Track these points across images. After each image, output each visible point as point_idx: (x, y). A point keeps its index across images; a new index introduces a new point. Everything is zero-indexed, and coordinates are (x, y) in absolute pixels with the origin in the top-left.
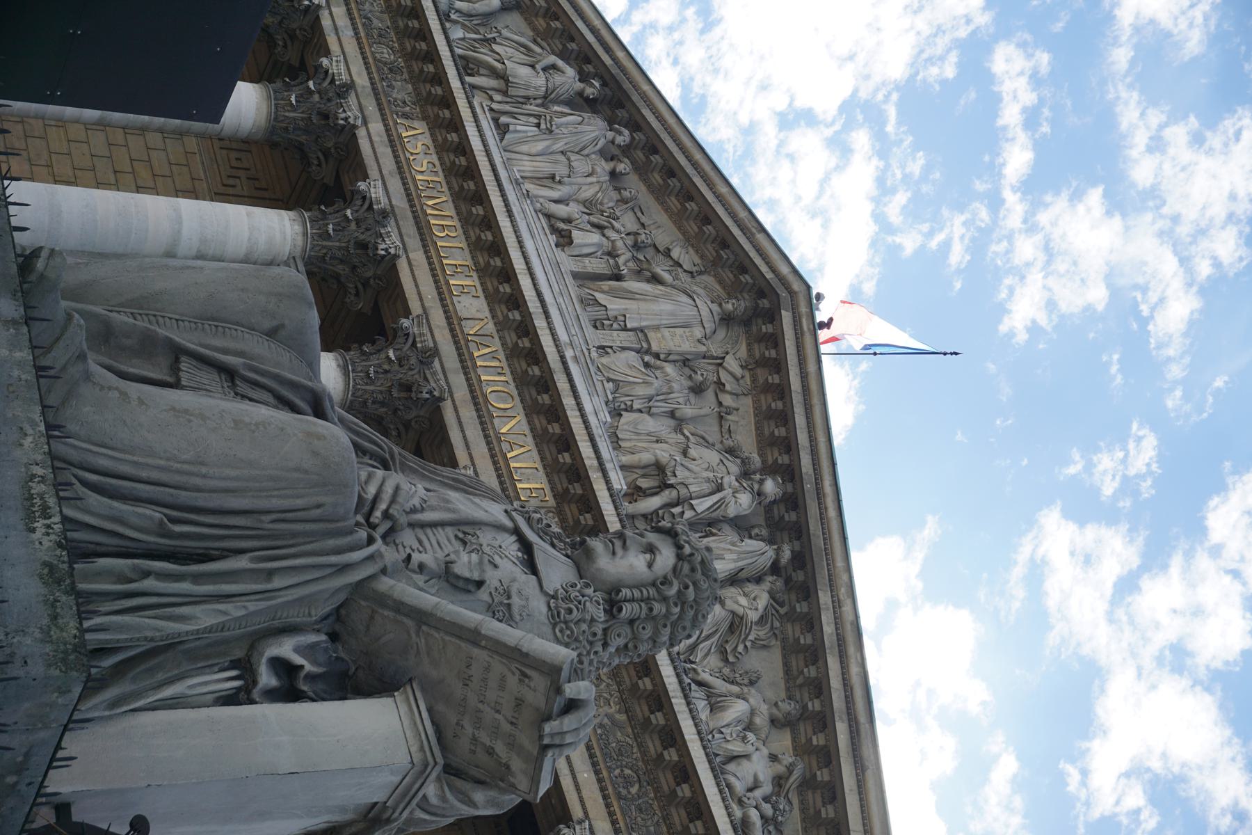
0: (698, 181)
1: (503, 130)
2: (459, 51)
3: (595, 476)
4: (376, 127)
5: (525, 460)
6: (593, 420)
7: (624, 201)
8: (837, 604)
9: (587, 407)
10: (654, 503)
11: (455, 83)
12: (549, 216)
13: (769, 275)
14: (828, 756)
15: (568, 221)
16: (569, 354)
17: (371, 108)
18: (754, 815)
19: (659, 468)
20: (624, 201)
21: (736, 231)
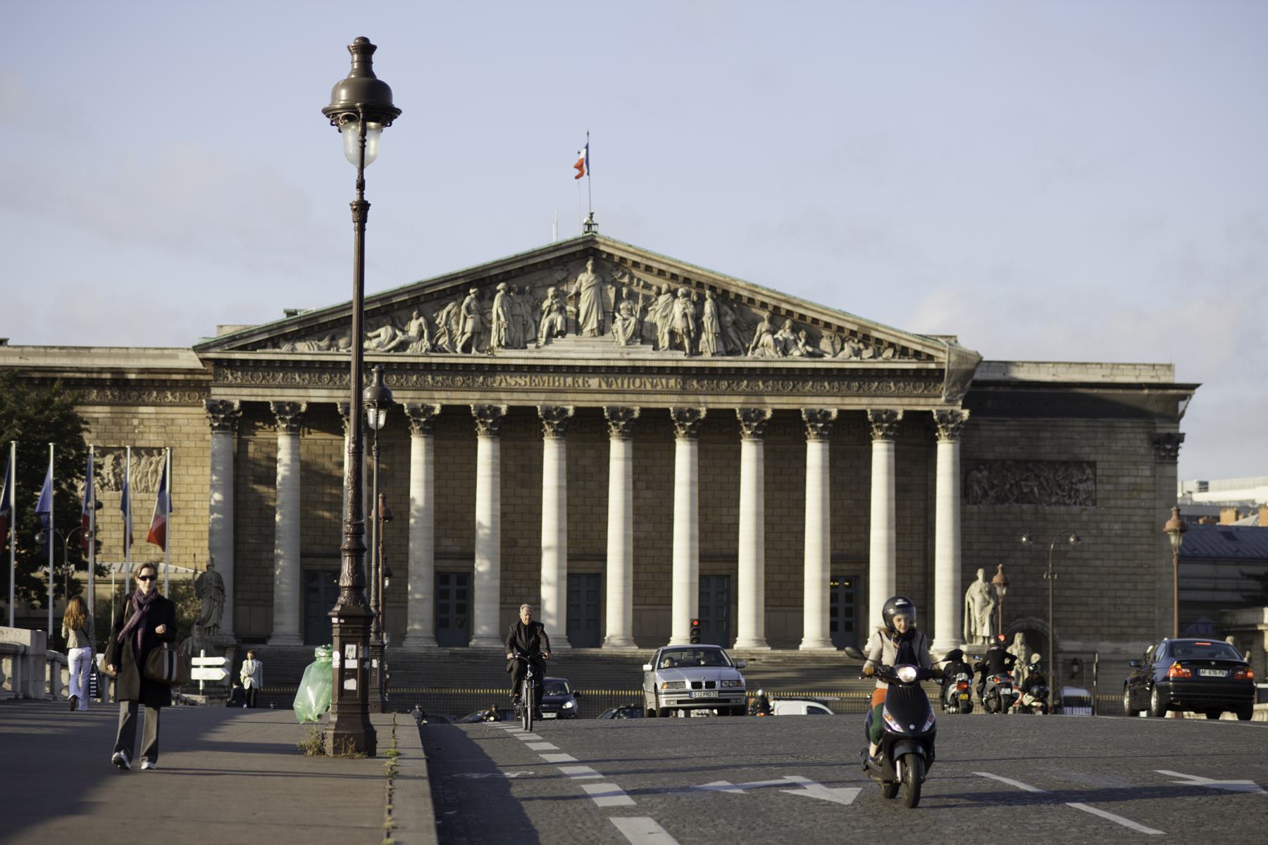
0: (531, 262)
1: (508, 346)
2: (459, 350)
3: (680, 364)
4: (503, 395)
5: (662, 382)
6: (655, 355)
7: (531, 293)
8: (737, 286)
9: (644, 354)
10: (686, 342)
11: (487, 361)
12: (550, 335)
13: (581, 248)
14: (789, 313)
15: (551, 327)
16: (626, 357)
17: (493, 395)
18: (810, 349)
19: (672, 333)
20: (531, 293)
21: (558, 254)
